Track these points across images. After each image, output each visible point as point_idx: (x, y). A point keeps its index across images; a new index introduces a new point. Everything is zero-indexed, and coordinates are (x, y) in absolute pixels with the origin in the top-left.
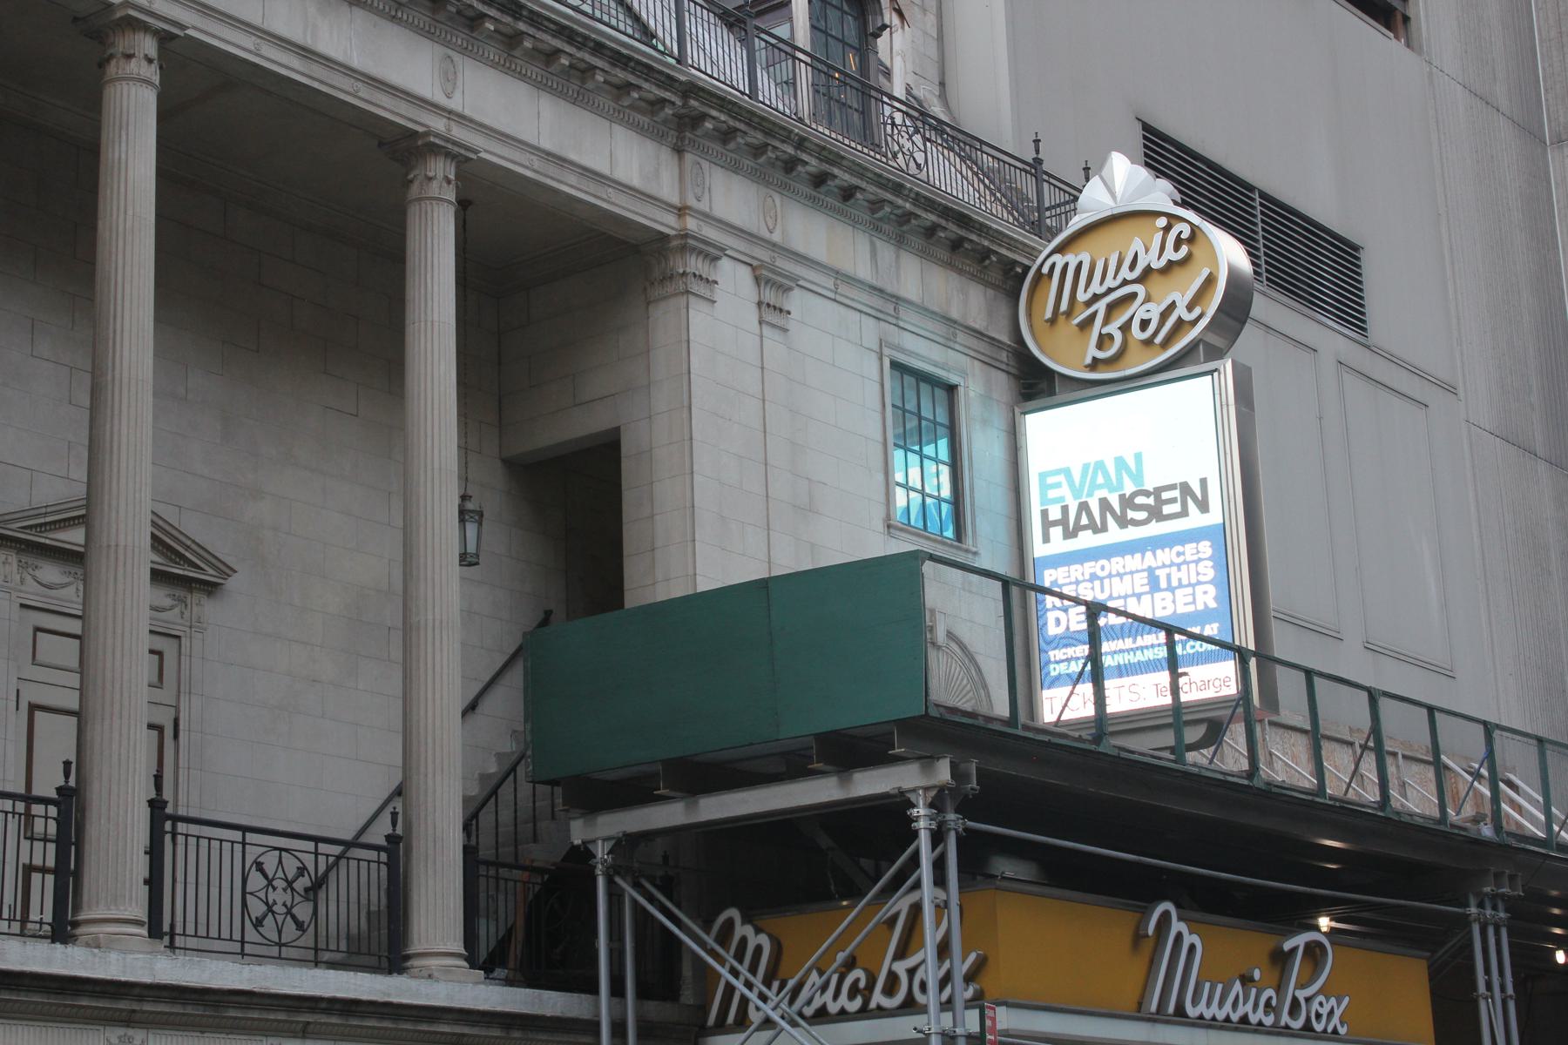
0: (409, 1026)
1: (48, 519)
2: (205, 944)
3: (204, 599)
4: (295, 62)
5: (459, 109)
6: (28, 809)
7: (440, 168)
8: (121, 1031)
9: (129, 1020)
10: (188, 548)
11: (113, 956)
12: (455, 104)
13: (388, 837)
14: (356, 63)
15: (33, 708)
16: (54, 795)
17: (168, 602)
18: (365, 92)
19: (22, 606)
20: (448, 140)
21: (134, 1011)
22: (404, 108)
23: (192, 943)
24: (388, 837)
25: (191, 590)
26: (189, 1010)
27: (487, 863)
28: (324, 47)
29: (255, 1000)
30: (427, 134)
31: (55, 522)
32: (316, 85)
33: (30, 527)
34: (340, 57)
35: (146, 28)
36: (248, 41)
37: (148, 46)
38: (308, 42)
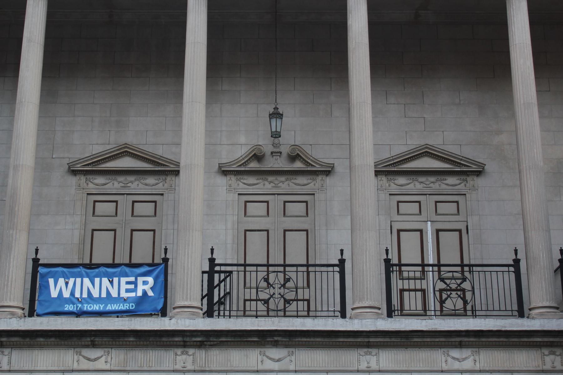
0: (526, 340)
2: (489, 313)
3: (475, 178)
6: (400, 269)
8: (366, 350)
9: (368, 345)
10: (461, 160)
11: (356, 321)
13: (514, 260)
15: (399, 231)
16: (512, 263)
17: (458, 182)
19: (390, 194)
21: (369, 342)
23: (483, 313)
24: (514, 260)
25: (468, 175)
26: (393, 340)
27: (396, 265)
29: (426, 334)
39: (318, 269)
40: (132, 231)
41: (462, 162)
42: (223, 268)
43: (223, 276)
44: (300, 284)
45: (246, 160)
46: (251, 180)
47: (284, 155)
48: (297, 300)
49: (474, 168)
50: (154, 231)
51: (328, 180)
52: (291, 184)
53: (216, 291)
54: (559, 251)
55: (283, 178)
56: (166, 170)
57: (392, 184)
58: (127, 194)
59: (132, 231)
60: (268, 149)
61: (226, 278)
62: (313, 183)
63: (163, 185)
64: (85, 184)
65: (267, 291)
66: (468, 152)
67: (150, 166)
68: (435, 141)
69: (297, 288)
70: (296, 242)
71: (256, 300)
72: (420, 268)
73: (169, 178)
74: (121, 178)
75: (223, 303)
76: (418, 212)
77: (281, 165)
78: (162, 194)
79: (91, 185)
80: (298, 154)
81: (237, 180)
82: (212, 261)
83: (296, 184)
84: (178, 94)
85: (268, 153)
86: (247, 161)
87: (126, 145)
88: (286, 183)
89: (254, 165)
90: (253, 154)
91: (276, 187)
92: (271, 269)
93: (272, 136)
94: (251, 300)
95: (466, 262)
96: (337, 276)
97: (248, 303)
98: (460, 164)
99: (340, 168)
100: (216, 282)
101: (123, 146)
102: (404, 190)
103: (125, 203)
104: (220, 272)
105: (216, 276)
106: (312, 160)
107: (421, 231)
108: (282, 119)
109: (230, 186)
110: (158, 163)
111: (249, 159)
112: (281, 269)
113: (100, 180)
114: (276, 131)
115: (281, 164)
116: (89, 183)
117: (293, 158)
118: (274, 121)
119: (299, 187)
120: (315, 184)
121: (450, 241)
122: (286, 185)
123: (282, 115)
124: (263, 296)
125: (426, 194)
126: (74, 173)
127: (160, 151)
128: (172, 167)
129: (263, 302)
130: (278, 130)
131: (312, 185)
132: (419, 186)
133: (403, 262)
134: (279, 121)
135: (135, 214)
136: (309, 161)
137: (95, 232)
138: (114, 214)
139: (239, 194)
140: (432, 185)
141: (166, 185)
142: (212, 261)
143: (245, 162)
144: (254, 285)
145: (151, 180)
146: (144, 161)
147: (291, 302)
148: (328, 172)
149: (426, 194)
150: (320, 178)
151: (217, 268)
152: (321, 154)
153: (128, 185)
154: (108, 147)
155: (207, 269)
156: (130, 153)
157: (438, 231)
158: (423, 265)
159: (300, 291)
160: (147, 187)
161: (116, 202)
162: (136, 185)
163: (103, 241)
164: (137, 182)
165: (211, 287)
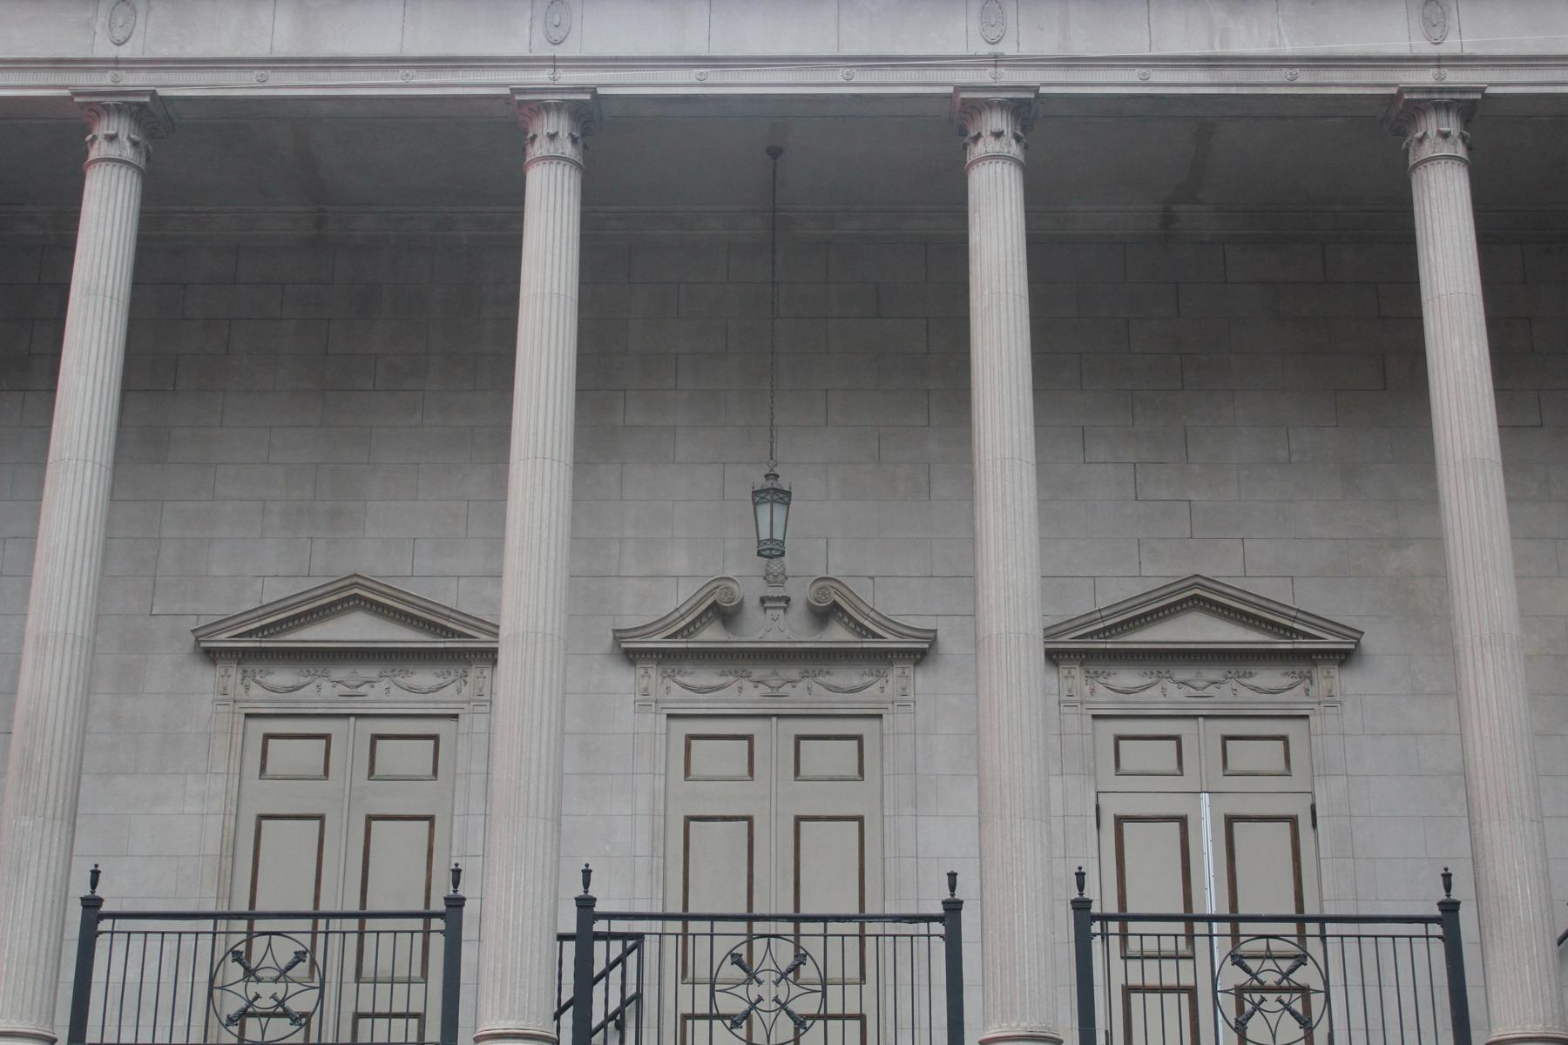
1: (1107, 623)
3: (1335, 671)
4: (1200, 76)
5: (1457, 51)
6: (1124, 928)
7: (1432, 125)
10: (1295, 619)
12: (1451, 46)
13: (1440, 904)
14: (1288, 49)
15: (1120, 821)
17: (1286, 681)
18: (1304, 76)
19: (1094, 717)
20: (1441, 90)
22: (1366, 76)
24: (1440, 904)
25: (1315, 664)
28: (1236, 49)
30: (1401, 91)
31: (1115, 626)
32: (1233, 90)
33: (1091, 634)
34: (1265, 50)
35: (989, 105)
36: (1133, 75)
37: (998, 121)
38: (1218, 50)
39: (891, 928)
40: (370, 818)
41: (1296, 626)
42: (619, 926)
43: (616, 948)
44: (834, 972)
45: (689, 619)
46: (705, 676)
47: (798, 607)
48: (826, 1017)
49: (1331, 642)
50: (430, 819)
51: (921, 680)
52: (816, 687)
53: (598, 991)
54: (1441, 880)
55: (793, 673)
56: (463, 648)
57: (1100, 689)
58: (358, 716)
59: (370, 818)
60: (750, 589)
61: (627, 952)
62: (877, 685)
63: (459, 691)
64: (240, 688)
65: (741, 990)
66: (1315, 598)
67: (423, 637)
68: (1225, 567)
69: (824, 983)
70: (829, 852)
71: (710, 1017)
72: (1180, 927)
73: (474, 672)
74: (341, 673)
75: (620, 1027)
76: (1174, 767)
77: (787, 634)
78: (456, 716)
79: (256, 691)
80: (835, 604)
81: (665, 675)
82: (585, 904)
83: (828, 688)
84: (496, 438)
85: (752, 603)
86: (693, 622)
87: (355, 580)
88: (802, 685)
89: (712, 635)
90: (709, 602)
91: (775, 696)
92: (759, 927)
93: (759, 554)
94: (374, 1015)
95: (1310, 909)
96: (940, 947)
97: (365, 1024)
98: (1292, 630)
99: (949, 644)
100: (599, 967)
101: (347, 582)
102: (1133, 704)
103: (350, 739)
104: (608, 937)
105: (599, 947)
106: (874, 621)
107: (1182, 821)
108: (788, 504)
109: (645, 693)
110: (443, 628)
111: (699, 617)
112: (788, 928)
113: (282, 677)
114: (772, 540)
115: (790, 630)
116: (253, 684)
117: (824, 614)
118: (764, 511)
119: (839, 696)
120: (882, 688)
121: (1264, 850)
122: (803, 690)
123: (789, 494)
124: (727, 1004)
125: (1196, 717)
126: (212, 656)
127: (451, 596)
128: (482, 641)
129: (728, 1022)
130: (778, 535)
131: (874, 689)
132: (1176, 693)
133: (1132, 909)
134: (779, 511)
135: (378, 771)
136: (866, 623)
137: (265, 823)
138: (321, 772)
139: (669, 716)
140: (1212, 690)
141: (466, 690)
142: (585, 904)
143: (687, 626)
144: (703, 972)
145: (424, 677)
146: (404, 623)
147: (809, 1023)
148: (920, 654)
149: (1196, 717)
150: (896, 671)
151: (600, 926)
152: (900, 604)
153: (362, 690)
154: (306, 585)
155: (573, 929)
156: (367, 600)
157: (1230, 820)
158: (1189, 919)
159: (834, 992)
160: (414, 697)
161: (326, 737)
162: (384, 691)
163: (289, 849)
164: (385, 683)
165: (586, 979)
